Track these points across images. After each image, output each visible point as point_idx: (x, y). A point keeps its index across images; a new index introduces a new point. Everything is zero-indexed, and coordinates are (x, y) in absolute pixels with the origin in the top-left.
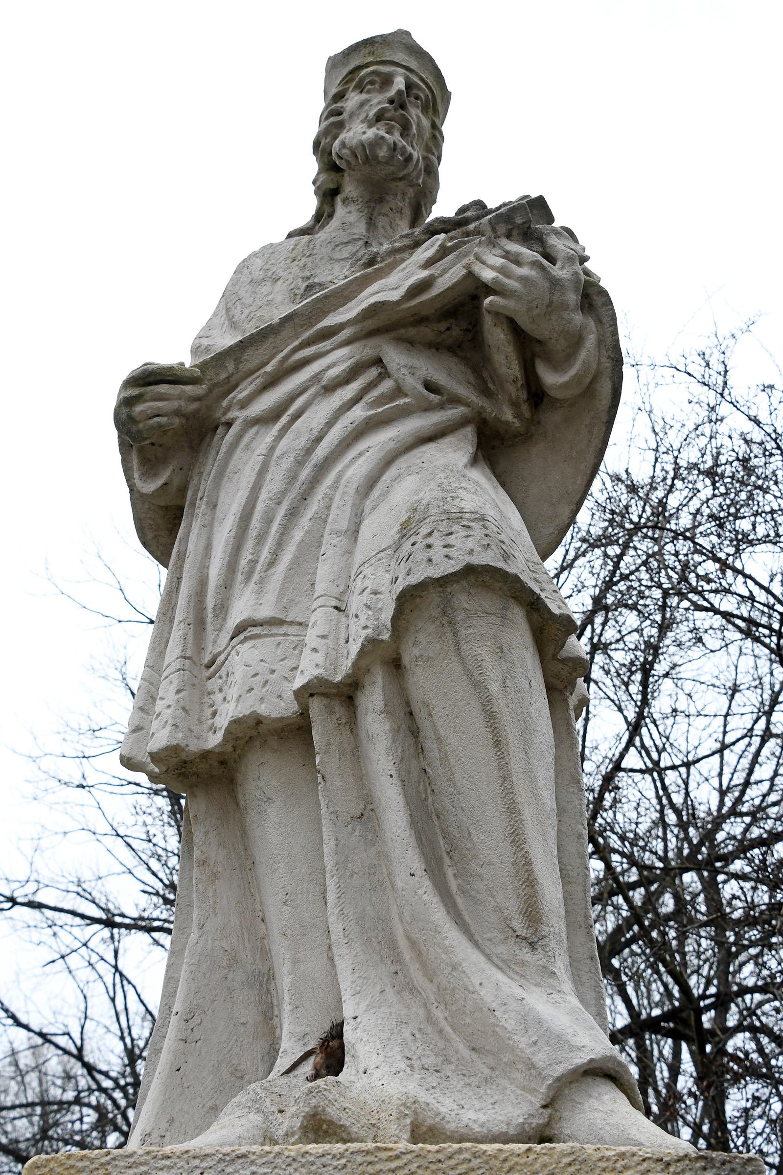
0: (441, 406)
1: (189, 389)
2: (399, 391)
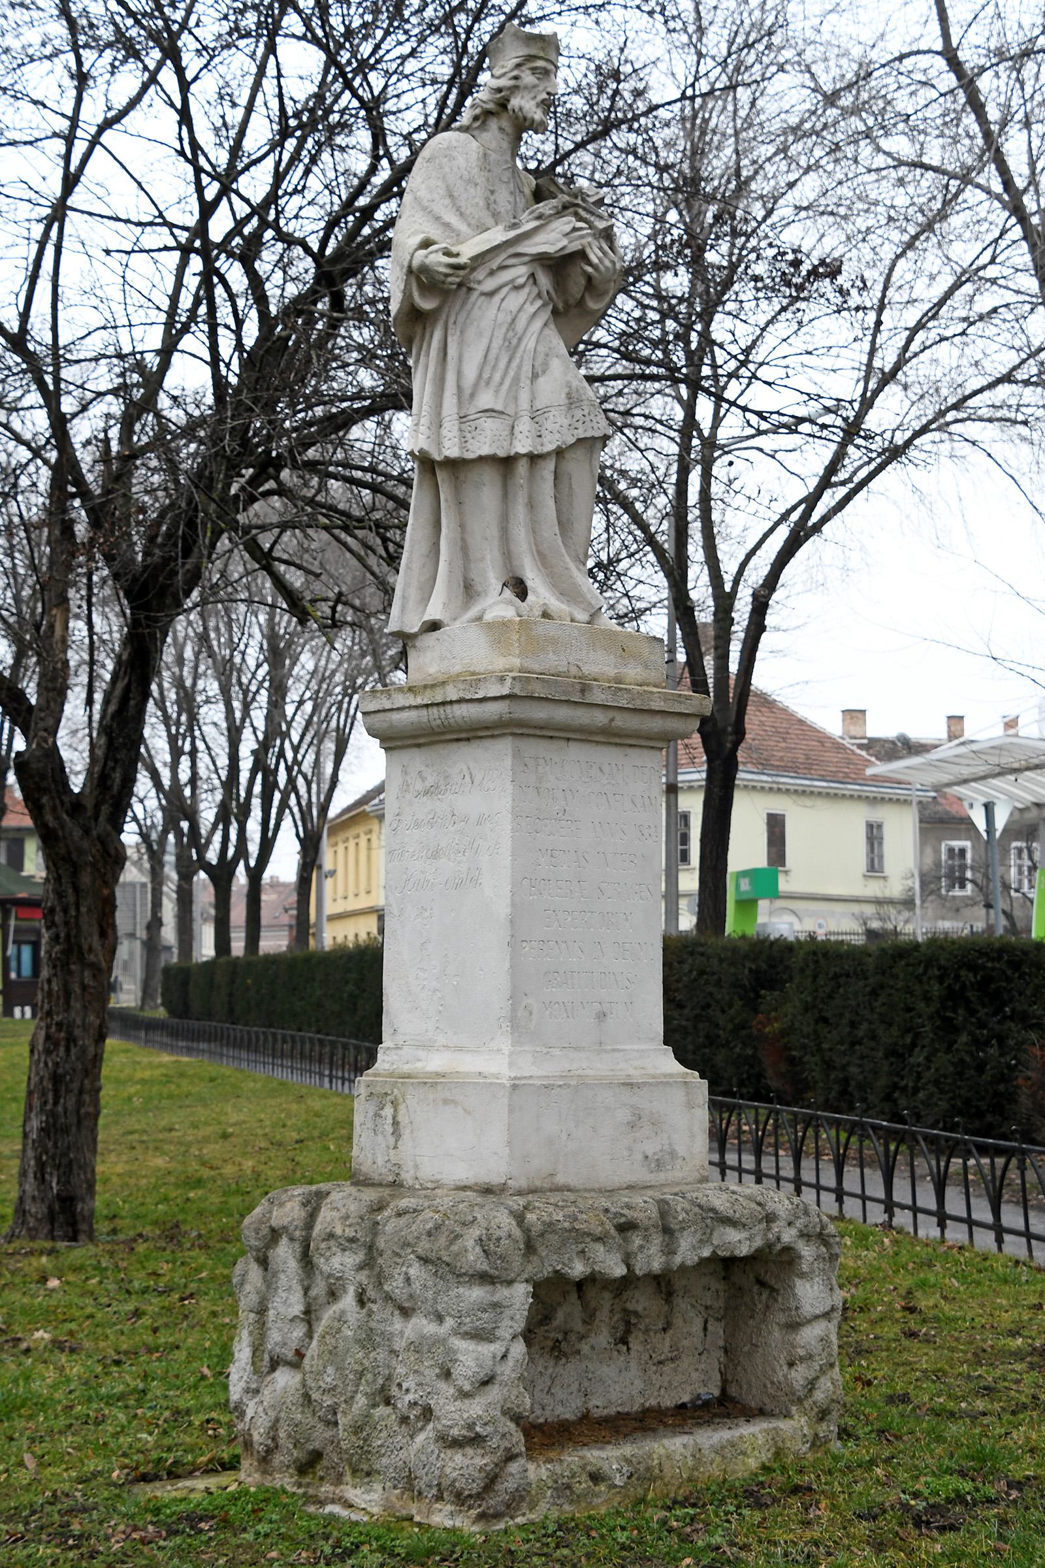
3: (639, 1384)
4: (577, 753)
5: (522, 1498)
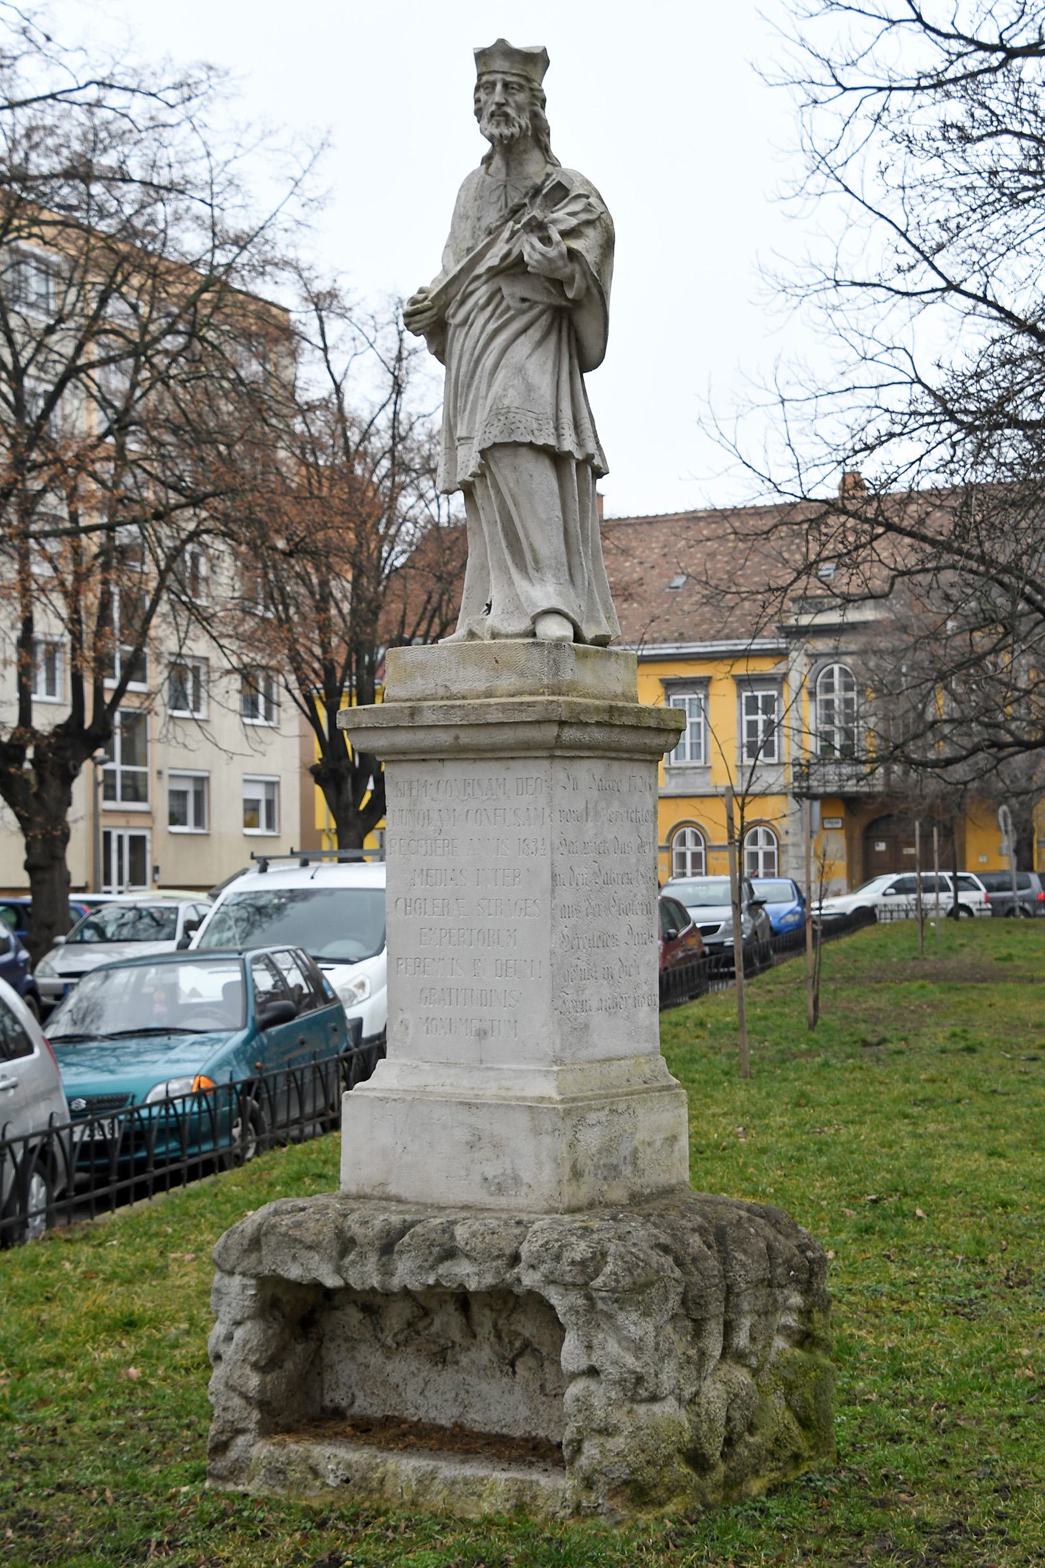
0: (530, 308)
1: (428, 314)
2: (508, 308)
3: (523, 1411)
4: (453, 772)
5: (242, 1470)
